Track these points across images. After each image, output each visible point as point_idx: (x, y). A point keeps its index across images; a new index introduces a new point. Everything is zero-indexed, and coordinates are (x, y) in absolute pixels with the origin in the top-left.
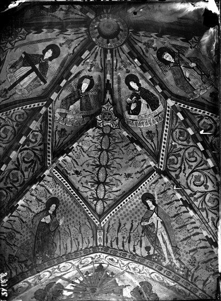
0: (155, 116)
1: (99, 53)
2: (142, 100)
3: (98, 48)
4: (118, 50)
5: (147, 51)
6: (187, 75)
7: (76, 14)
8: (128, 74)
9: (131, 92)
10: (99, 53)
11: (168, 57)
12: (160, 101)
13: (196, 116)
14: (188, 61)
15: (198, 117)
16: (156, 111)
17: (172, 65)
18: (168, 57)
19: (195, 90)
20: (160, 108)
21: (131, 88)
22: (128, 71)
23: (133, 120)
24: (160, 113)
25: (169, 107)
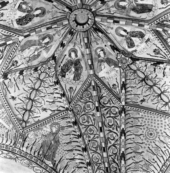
0: (12, 21)
1: (70, 3)
2: (26, 14)
3: (74, 4)
4: (65, 13)
5: (55, 30)
6: (32, 48)
7: (103, 10)
8: (47, 11)
9: (34, 9)
10: (70, 3)
11: (47, 40)
12: (21, 26)
13: (4, 48)
14: (39, 51)
15: (3, 50)
16: (15, 23)
17: (41, 41)
18: (47, 40)
19: (22, 52)
20: (16, 26)
21: (37, 9)
22: (49, 12)
23: (15, 5)
24: (13, 25)
25: (18, 36)
